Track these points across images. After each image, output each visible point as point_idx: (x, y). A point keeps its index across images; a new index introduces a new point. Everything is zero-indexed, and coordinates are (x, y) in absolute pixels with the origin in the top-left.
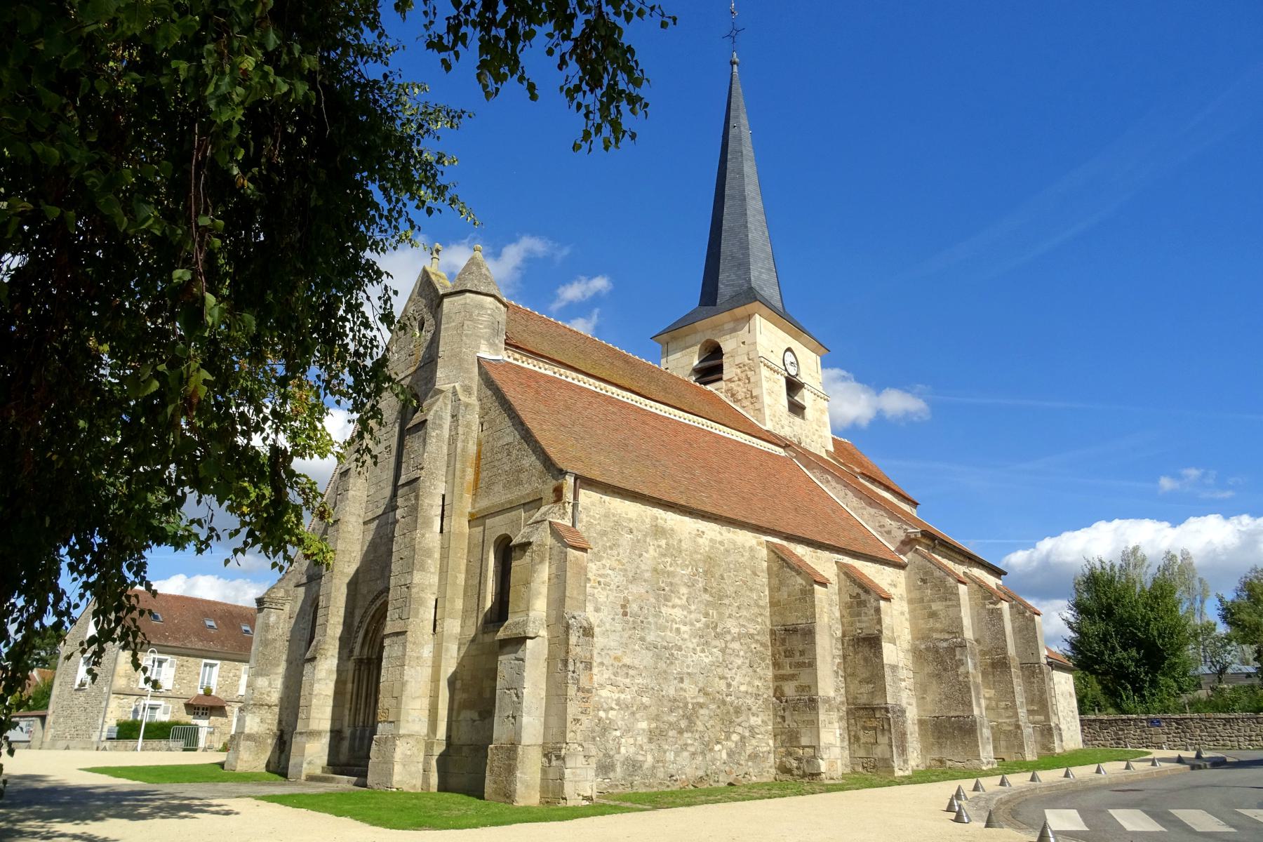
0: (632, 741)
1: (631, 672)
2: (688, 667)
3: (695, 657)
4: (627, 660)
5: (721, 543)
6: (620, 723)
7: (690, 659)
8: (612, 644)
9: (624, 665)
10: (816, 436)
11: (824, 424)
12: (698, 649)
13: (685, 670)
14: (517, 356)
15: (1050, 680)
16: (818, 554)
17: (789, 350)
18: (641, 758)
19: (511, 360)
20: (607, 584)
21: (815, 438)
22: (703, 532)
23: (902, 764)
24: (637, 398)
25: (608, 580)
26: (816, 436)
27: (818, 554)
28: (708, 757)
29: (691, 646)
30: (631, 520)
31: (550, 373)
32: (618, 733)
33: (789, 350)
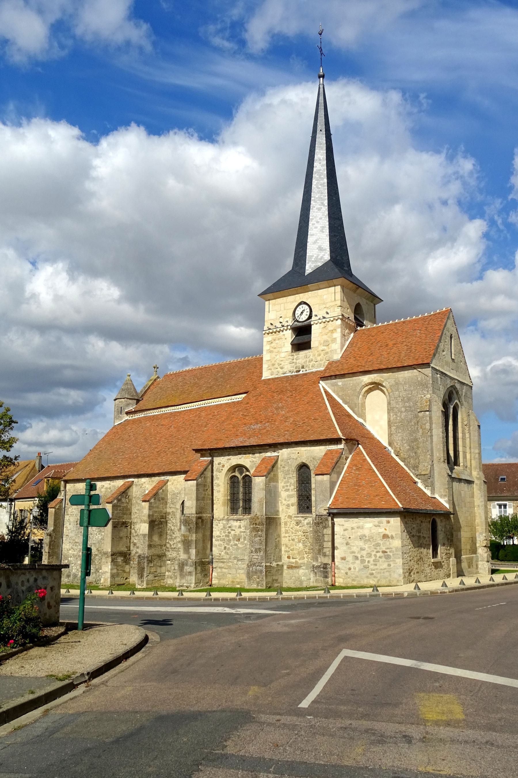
0: (75, 567)
1: (77, 544)
2: (94, 541)
3: (97, 537)
4: (76, 541)
5: (110, 488)
6: (73, 562)
7: (94, 538)
8: (73, 535)
9: (76, 542)
10: (322, 355)
11: (334, 340)
12: (98, 533)
13: (93, 542)
14: (131, 415)
15: (325, 527)
16: (153, 479)
17: (300, 304)
18: (77, 573)
19: (131, 418)
20: (73, 515)
21: (319, 358)
22: (104, 486)
23: (140, 582)
24: (173, 408)
25: (73, 513)
26: (322, 355)
27: (153, 479)
28: (98, 574)
29: (95, 533)
30: (81, 489)
31: (143, 415)
32: (73, 565)
33: (300, 304)
